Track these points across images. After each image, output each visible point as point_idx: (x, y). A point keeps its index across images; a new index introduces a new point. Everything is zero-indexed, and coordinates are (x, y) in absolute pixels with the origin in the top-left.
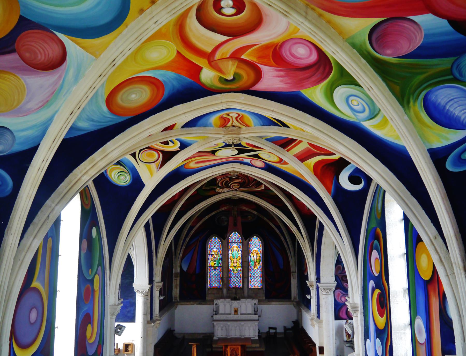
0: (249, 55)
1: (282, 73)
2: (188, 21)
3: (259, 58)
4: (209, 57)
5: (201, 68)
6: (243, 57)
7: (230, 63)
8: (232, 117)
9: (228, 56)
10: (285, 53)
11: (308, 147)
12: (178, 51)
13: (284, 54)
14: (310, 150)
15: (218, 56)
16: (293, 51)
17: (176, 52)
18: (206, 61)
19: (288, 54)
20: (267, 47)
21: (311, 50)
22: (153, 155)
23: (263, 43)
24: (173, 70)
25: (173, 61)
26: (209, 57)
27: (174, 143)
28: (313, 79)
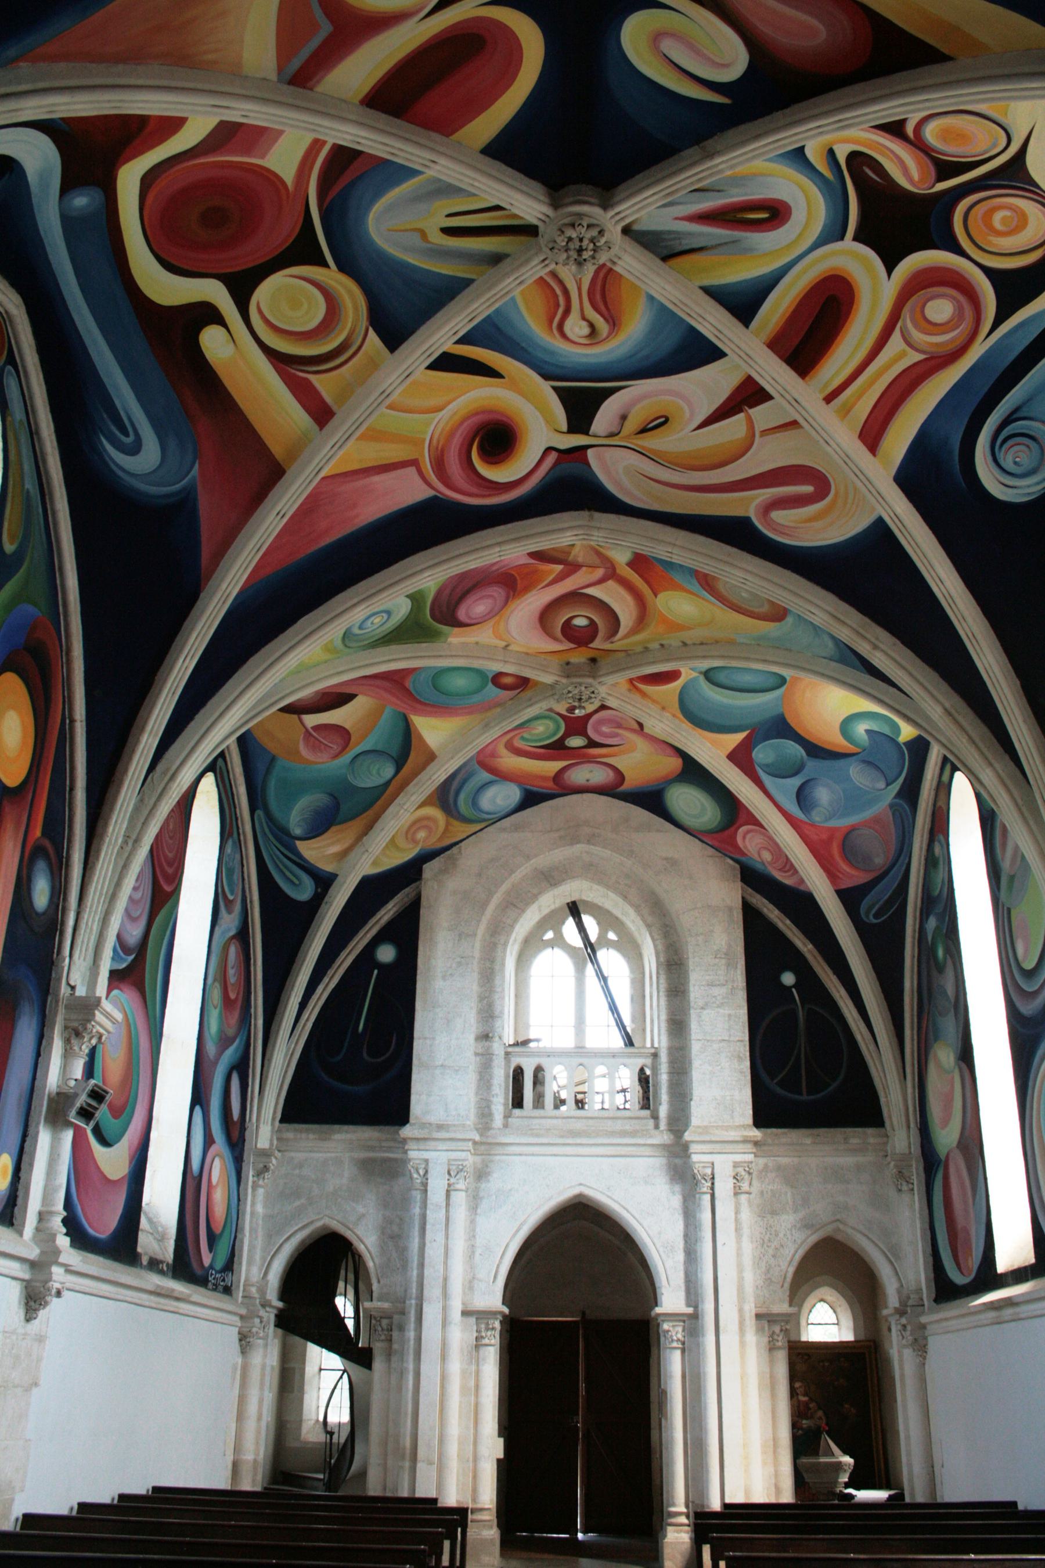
0: (551, 572)
1: (494, 568)
2: (631, 624)
3: (536, 571)
4: (612, 574)
5: (630, 564)
6: (560, 567)
7: (580, 560)
8: (584, 318)
9: (584, 569)
10: (497, 592)
11: (263, 157)
12: (656, 596)
13: (500, 590)
14: (248, 152)
15: (599, 573)
16: (490, 601)
17: (659, 596)
18: (618, 571)
19: (495, 594)
20: (526, 589)
21: (470, 618)
22: (945, 134)
23: (534, 592)
24: (672, 579)
25: (666, 589)
26: (612, 574)
27: (831, 153)
28: (447, 591)
